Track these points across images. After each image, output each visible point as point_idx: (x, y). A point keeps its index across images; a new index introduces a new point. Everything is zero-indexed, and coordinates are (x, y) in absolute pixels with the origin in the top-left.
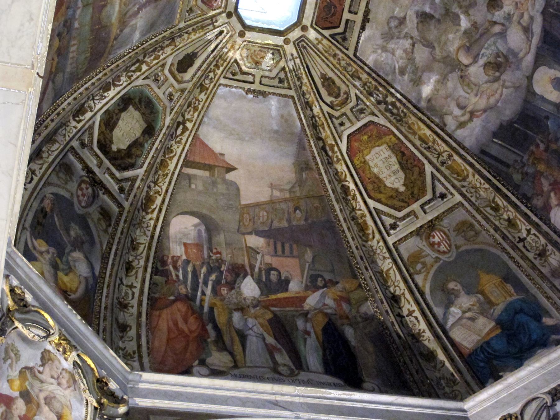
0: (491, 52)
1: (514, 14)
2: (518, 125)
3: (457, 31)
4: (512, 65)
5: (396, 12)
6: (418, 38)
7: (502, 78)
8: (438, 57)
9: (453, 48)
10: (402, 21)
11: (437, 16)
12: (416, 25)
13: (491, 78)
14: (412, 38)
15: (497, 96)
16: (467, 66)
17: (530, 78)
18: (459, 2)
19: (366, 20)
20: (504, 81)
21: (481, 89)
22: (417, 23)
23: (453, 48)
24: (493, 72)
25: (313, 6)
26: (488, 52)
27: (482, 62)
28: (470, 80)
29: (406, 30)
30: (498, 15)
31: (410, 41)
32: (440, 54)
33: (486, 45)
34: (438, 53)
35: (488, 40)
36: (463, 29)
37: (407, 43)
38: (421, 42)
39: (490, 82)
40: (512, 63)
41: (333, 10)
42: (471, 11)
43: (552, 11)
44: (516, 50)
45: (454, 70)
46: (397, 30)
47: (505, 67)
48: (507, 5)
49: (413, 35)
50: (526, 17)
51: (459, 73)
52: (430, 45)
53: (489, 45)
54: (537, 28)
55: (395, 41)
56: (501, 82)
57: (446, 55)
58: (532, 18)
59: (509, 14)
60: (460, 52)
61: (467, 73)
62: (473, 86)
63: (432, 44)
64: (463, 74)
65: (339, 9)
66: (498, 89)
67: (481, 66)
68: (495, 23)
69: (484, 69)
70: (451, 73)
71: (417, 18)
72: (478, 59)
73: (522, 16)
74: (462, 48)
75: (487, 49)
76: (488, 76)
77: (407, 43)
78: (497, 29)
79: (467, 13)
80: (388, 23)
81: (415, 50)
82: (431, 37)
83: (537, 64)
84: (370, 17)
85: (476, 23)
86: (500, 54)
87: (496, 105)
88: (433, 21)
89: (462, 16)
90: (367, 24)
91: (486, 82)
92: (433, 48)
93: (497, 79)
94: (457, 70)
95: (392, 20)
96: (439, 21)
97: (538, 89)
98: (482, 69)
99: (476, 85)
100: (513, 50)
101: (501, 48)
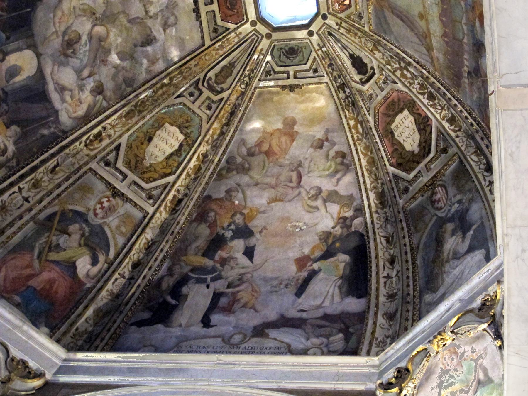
0: (81, 51)
1: (79, 94)
2: (28, 12)
3: (117, 48)
4: (58, 54)
5: (174, 30)
6: (145, 21)
7: (61, 38)
8: (122, 15)
9: (113, 32)
10: (165, 26)
11: (139, 49)
12: (153, 30)
13: (70, 31)
14: (151, 17)
15: (57, 20)
16: (94, 25)
17: (39, 55)
18: (126, 71)
19: (197, 10)
20: (58, 37)
21: (73, 16)
22: (152, 32)
23: (113, 32)
24: (71, 37)
25: (247, 4)
26: (84, 49)
27: (84, 38)
28: (85, 16)
29: (159, 20)
30: (90, 84)
31: (151, 14)
32: (121, 20)
33: (87, 54)
34: (123, 19)
35: (88, 59)
36: (113, 52)
37: (153, 10)
38: (142, 19)
39: (68, 28)
40: (60, 56)
41: (228, 4)
42: (113, 70)
43: (52, 119)
44: (62, 68)
45: (103, 15)
46: (166, 16)
47: (63, 49)
48: (87, 96)
49: (151, 20)
50: (68, 98)
51: (97, 15)
52: (132, 21)
53: (85, 56)
54: (55, 97)
55: (164, 6)
56: (60, 34)
57: (116, 23)
58: (63, 101)
59: (82, 90)
60: (106, 32)
61: (91, 20)
62: (80, 13)
63: (132, 24)
64: (94, 17)
65: (223, 7)
66: (59, 27)
67: (82, 34)
68: (89, 76)
69: (79, 34)
70: (104, 11)
71: (154, 36)
72: (88, 38)
73: (72, 97)
74: (105, 36)
75: (85, 52)
76: (72, 31)
77: (153, 10)
78: (86, 73)
79: (116, 67)
80: (176, 17)
81: (143, 8)
82: (135, 29)
83: (40, 71)
84: (194, 15)
85: (105, 65)
86: (72, 55)
87: (54, 12)
88: (140, 44)
89: (118, 62)
90: (194, 7)
91: (72, 24)
92: (129, 21)
93: (65, 33)
94: (101, 16)
95: (174, 22)
96: (135, 46)
97: (28, 53)
98: (81, 33)
99: (80, 15)
100: (64, 66)
101: (75, 60)
